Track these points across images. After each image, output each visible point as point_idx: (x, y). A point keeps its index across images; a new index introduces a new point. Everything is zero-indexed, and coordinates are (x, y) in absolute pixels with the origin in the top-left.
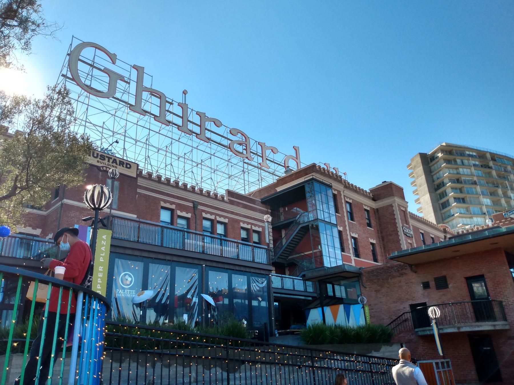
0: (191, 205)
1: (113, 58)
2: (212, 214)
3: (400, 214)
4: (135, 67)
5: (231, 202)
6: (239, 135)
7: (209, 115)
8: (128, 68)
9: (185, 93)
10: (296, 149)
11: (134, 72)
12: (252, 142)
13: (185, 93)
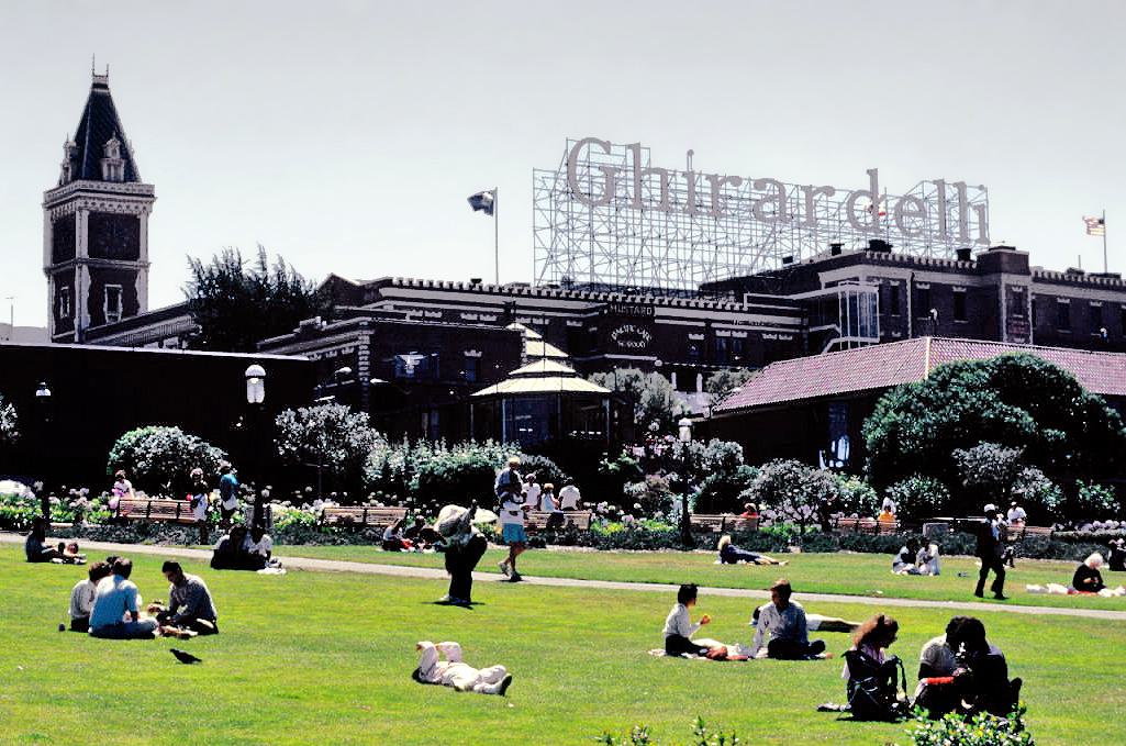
0: (702, 324)
1: (607, 146)
2: (726, 330)
3: (1008, 300)
4: (629, 147)
5: (751, 311)
6: (768, 185)
7: (722, 172)
8: (622, 151)
9: (690, 153)
10: (873, 173)
11: (630, 153)
12: (788, 189)
13: (690, 153)
